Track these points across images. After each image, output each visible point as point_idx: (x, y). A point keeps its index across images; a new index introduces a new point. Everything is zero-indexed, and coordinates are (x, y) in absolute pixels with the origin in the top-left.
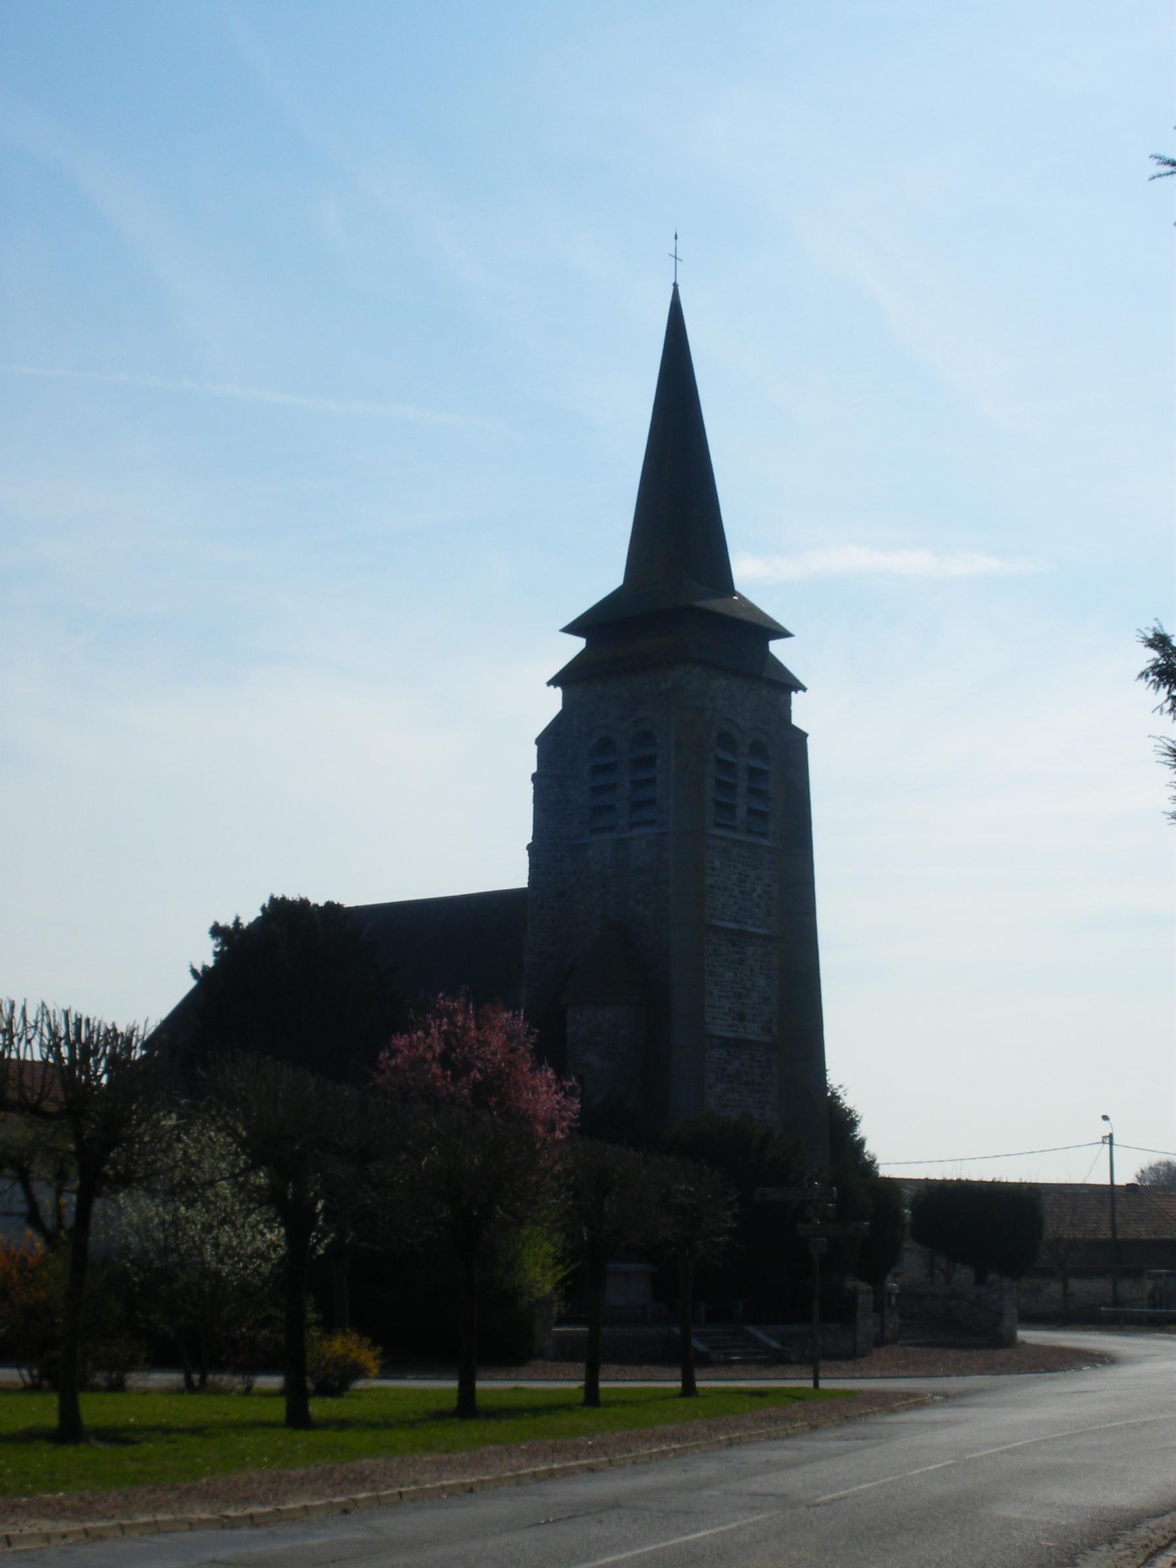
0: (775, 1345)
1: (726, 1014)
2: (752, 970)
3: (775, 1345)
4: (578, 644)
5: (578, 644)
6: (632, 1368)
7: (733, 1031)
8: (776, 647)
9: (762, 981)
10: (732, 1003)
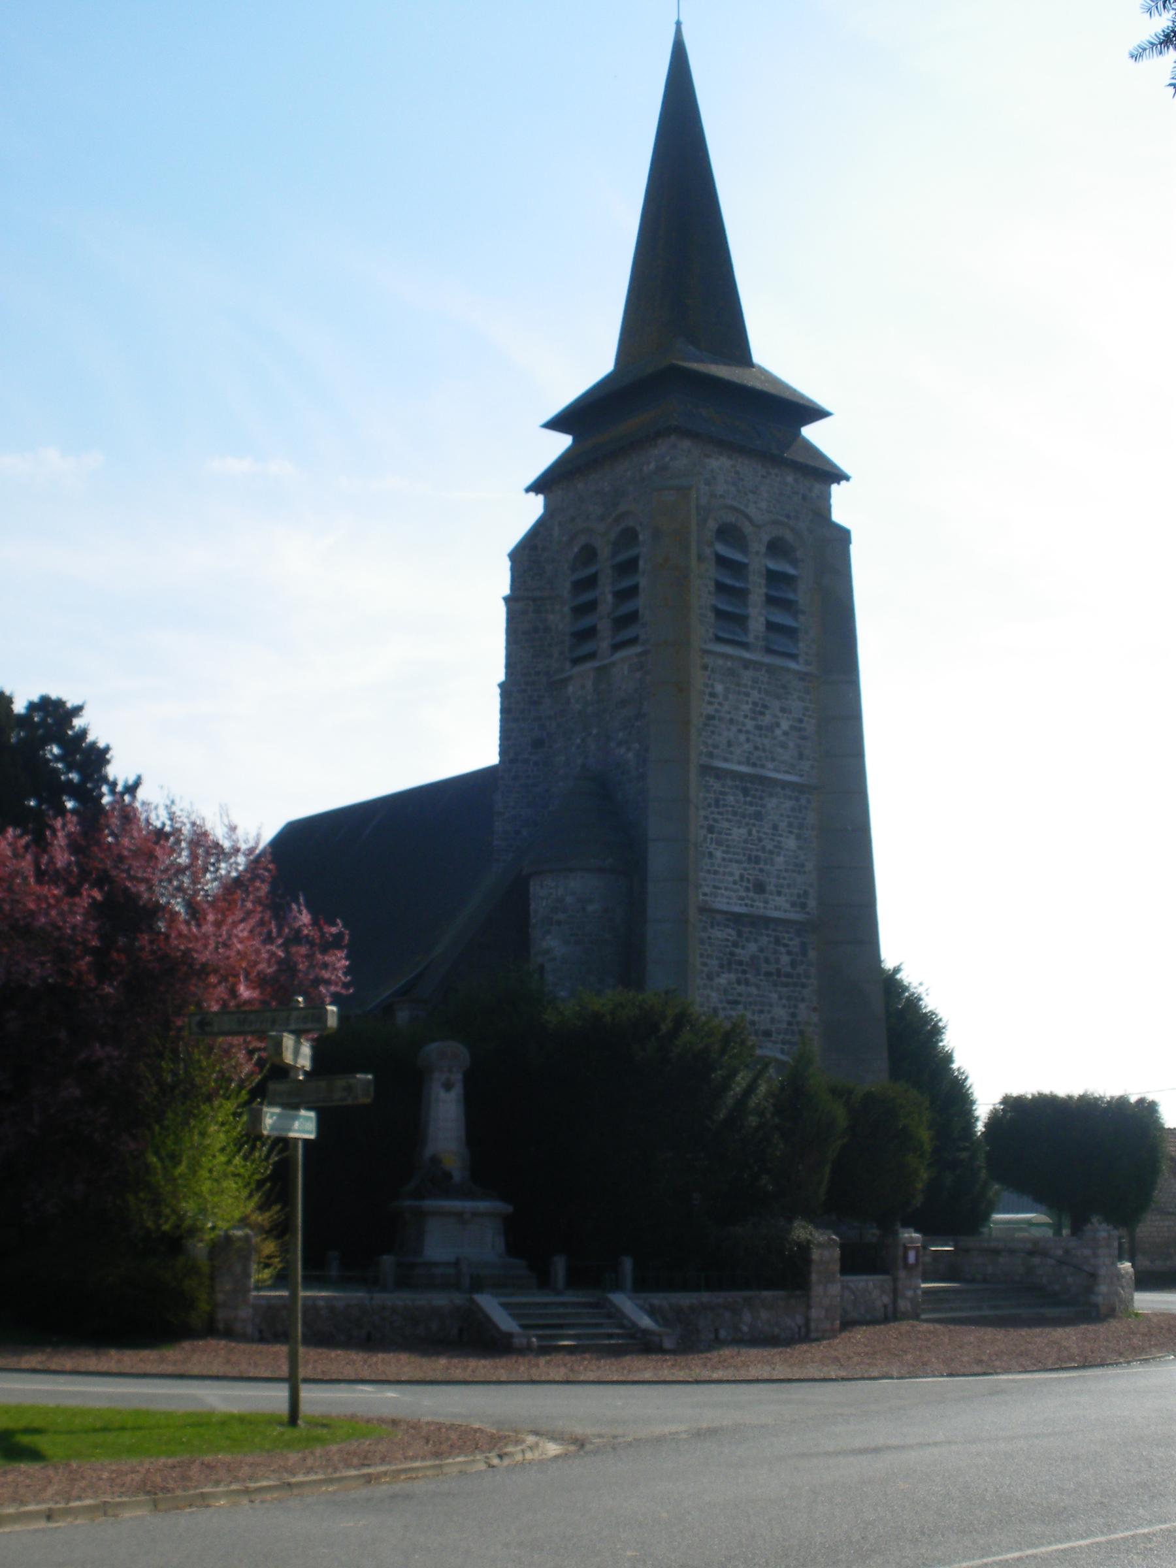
0: (646, 1322)
1: (735, 883)
2: (775, 827)
3: (646, 1322)
4: (562, 442)
5: (562, 442)
6: (233, 1344)
7: (746, 905)
8: (811, 432)
9: (791, 843)
10: (745, 869)
